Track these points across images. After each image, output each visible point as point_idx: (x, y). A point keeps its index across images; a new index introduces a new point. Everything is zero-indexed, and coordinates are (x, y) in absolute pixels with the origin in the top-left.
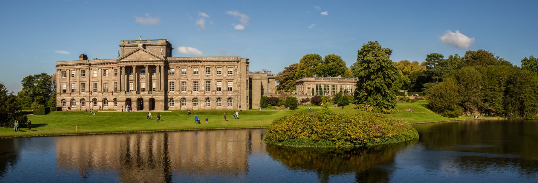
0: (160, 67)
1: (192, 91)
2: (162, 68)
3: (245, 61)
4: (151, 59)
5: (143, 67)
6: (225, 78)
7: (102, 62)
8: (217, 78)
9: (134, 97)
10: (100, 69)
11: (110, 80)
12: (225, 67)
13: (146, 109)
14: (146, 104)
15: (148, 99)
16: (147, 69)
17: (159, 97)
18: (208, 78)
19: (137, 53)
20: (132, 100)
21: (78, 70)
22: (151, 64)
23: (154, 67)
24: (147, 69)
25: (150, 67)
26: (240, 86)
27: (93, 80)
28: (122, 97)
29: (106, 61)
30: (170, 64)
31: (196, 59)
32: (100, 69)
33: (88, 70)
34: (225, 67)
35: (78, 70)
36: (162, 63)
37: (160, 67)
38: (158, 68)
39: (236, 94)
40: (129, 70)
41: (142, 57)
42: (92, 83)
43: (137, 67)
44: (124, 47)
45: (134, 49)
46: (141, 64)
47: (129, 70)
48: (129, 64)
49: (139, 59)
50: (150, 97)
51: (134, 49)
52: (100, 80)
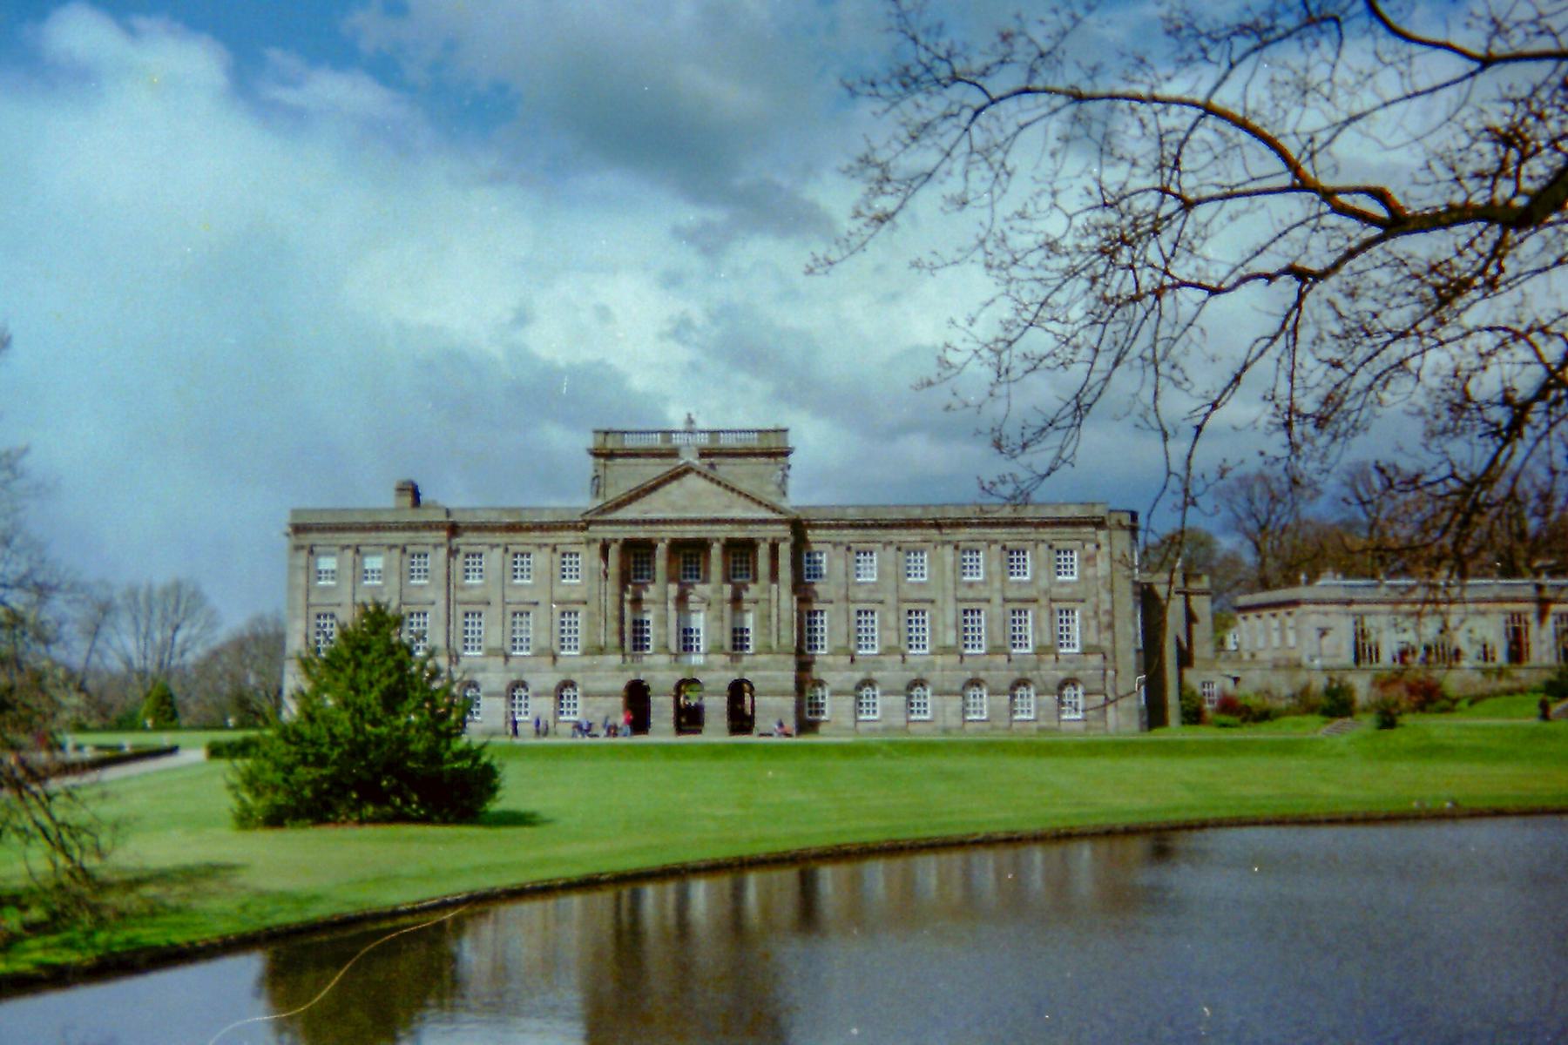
0: (774, 548)
1: (904, 647)
2: (785, 549)
3: (1126, 520)
4: (738, 513)
5: (702, 546)
6: (1046, 592)
7: (507, 519)
8: (1010, 595)
9: (660, 672)
10: (499, 551)
11: (543, 598)
12: (1043, 547)
13: (716, 730)
14: (715, 706)
15: (724, 686)
16: (716, 551)
17: (772, 677)
18: (971, 594)
19: (675, 484)
20: (654, 688)
21: (397, 552)
22: (739, 533)
23: (749, 546)
24: (716, 551)
25: (731, 546)
26: (1111, 626)
27: (461, 595)
28: (612, 676)
29: (528, 518)
30: (811, 535)
31: (917, 513)
32: (499, 551)
33: (443, 552)
34: (1043, 547)
35: (397, 552)
36: (783, 531)
37: (774, 548)
38: (763, 551)
39: (1095, 660)
40: (636, 556)
41: (692, 503)
42: (460, 610)
43: (677, 546)
44: (611, 455)
45: (654, 469)
46: (691, 532)
47: (636, 556)
48: (641, 533)
49: (684, 508)
50: (733, 675)
51: (654, 469)
52: (496, 598)
